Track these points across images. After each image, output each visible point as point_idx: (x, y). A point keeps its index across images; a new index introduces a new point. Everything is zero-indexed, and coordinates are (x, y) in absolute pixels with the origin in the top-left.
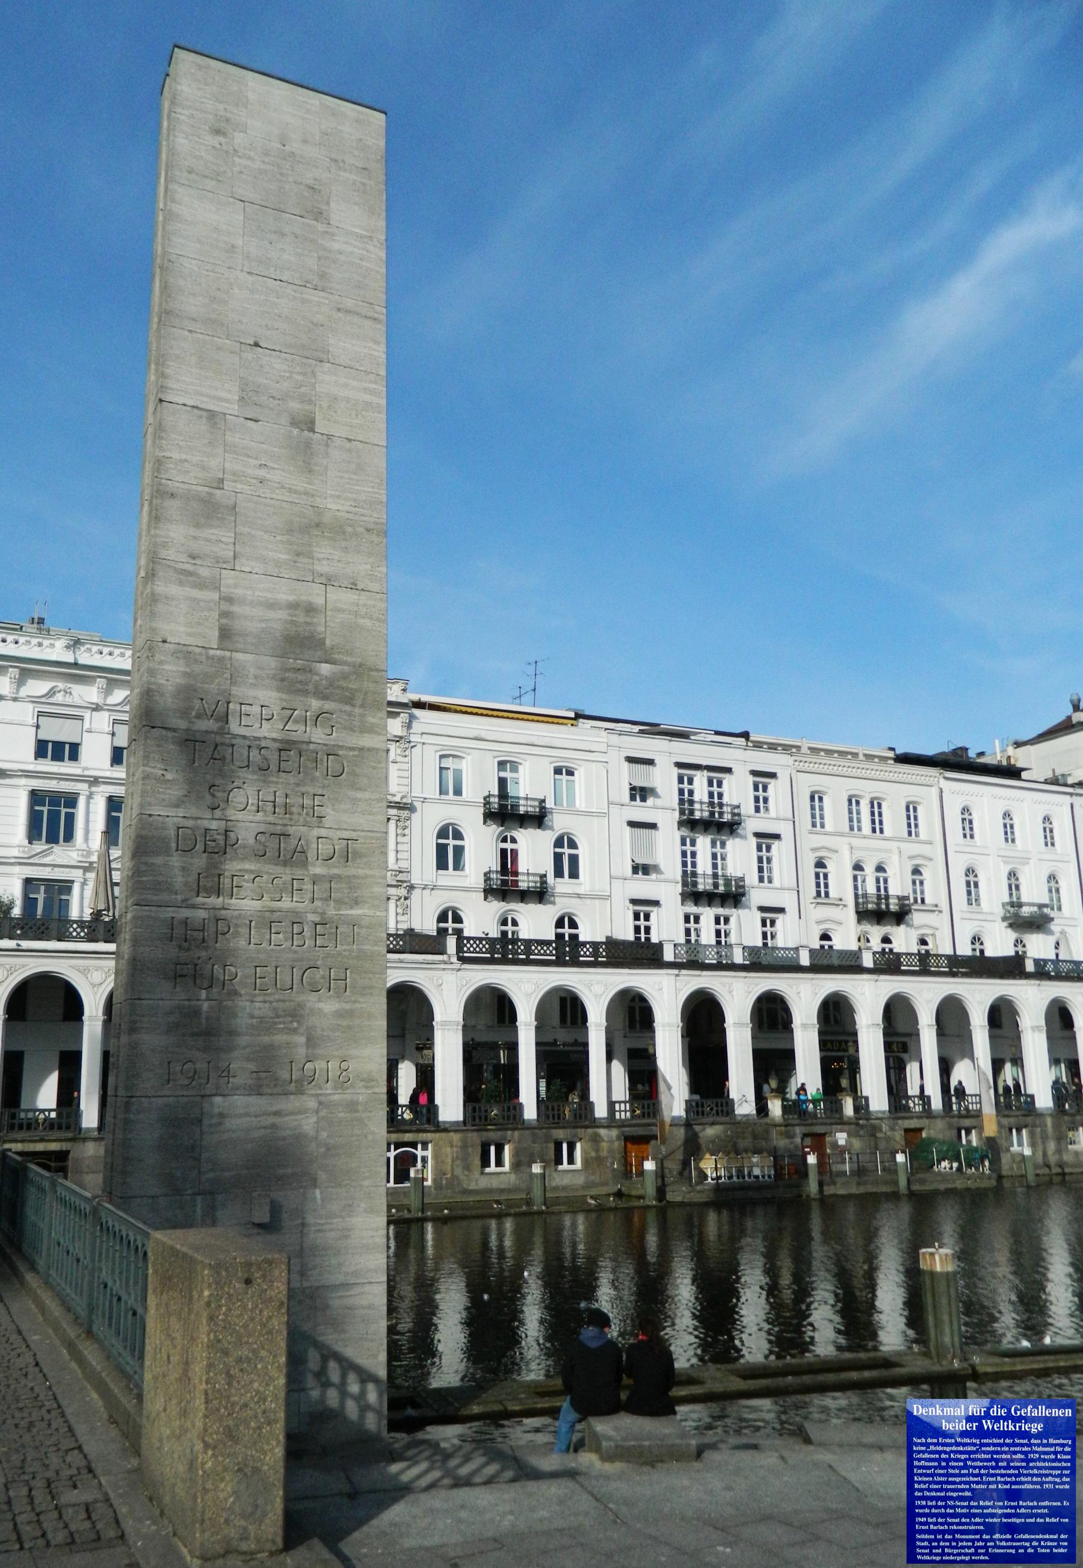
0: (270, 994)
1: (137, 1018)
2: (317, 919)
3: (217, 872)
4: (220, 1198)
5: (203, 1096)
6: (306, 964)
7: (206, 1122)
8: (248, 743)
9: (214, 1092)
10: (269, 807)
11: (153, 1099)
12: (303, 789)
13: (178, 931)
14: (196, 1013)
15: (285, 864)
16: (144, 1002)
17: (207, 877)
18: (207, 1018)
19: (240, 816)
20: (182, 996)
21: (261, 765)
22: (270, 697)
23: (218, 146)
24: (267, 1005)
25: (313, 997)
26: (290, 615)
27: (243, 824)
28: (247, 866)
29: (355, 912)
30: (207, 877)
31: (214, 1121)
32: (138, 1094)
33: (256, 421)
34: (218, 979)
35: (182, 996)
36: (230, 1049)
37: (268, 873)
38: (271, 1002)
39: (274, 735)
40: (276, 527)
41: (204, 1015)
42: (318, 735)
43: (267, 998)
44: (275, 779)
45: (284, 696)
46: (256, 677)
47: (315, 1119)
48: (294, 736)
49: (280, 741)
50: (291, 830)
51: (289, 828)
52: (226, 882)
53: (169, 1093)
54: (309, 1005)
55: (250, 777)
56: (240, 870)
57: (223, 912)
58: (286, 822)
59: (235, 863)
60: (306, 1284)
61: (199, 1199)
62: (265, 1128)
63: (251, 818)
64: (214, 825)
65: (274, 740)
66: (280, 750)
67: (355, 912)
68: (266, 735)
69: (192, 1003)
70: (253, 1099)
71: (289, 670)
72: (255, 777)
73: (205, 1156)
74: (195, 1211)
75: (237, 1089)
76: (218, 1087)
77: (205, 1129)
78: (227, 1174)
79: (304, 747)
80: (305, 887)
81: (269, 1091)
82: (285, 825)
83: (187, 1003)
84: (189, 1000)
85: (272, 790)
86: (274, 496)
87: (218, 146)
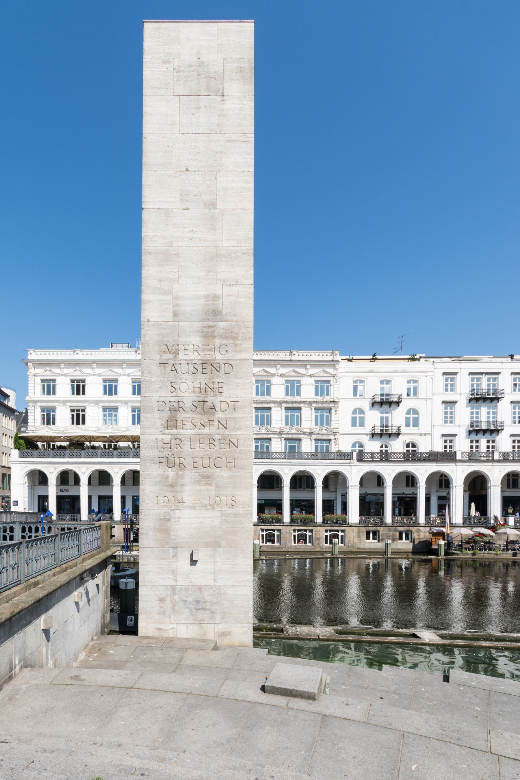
0: (199, 469)
1: (144, 479)
2: (220, 437)
3: (175, 419)
4: (179, 549)
5: (171, 510)
6: (215, 456)
7: (172, 520)
8: (187, 362)
9: (176, 508)
10: (197, 390)
11: (151, 511)
12: (213, 381)
13: (160, 444)
14: (167, 477)
15: (205, 414)
16: (146, 473)
17: (170, 421)
18: (172, 479)
19: (184, 394)
20: (161, 470)
21: (193, 372)
22: (198, 340)
23: (166, 70)
24: (198, 474)
25: (218, 470)
26: (205, 301)
27: (185, 398)
28: (187, 415)
29: (237, 433)
30: (170, 421)
31: (176, 520)
32: (145, 509)
33: (188, 209)
34: (177, 464)
35: (161, 470)
36: (182, 492)
37: (196, 418)
38: (199, 472)
39: (199, 357)
40: (198, 260)
41: (170, 478)
42: (219, 356)
43: (198, 471)
44: (199, 377)
45: (203, 339)
46: (190, 332)
47: (220, 520)
48: (208, 357)
49: (202, 360)
50: (206, 399)
51: (207, 398)
52: (179, 423)
53: (157, 509)
54: (216, 473)
55: (188, 377)
56: (185, 418)
57: (177, 436)
58: (205, 396)
59: (183, 415)
60: (216, 584)
61: (171, 549)
62: (198, 523)
63: (189, 395)
64: (172, 399)
65: (199, 360)
66: (202, 364)
67: (237, 433)
68: (195, 358)
69: (166, 473)
70: (193, 512)
71: (205, 327)
72: (190, 377)
73: (172, 533)
74: (169, 554)
75: (186, 507)
76: (177, 506)
77: (172, 523)
78: (182, 540)
79: (213, 362)
80: (214, 423)
81: (199, 509)
82: (205, 397)
83: (163, 473)
84: (164, 472)
85: (198, 382)
86: (197, 245)
87: (166, 70)
